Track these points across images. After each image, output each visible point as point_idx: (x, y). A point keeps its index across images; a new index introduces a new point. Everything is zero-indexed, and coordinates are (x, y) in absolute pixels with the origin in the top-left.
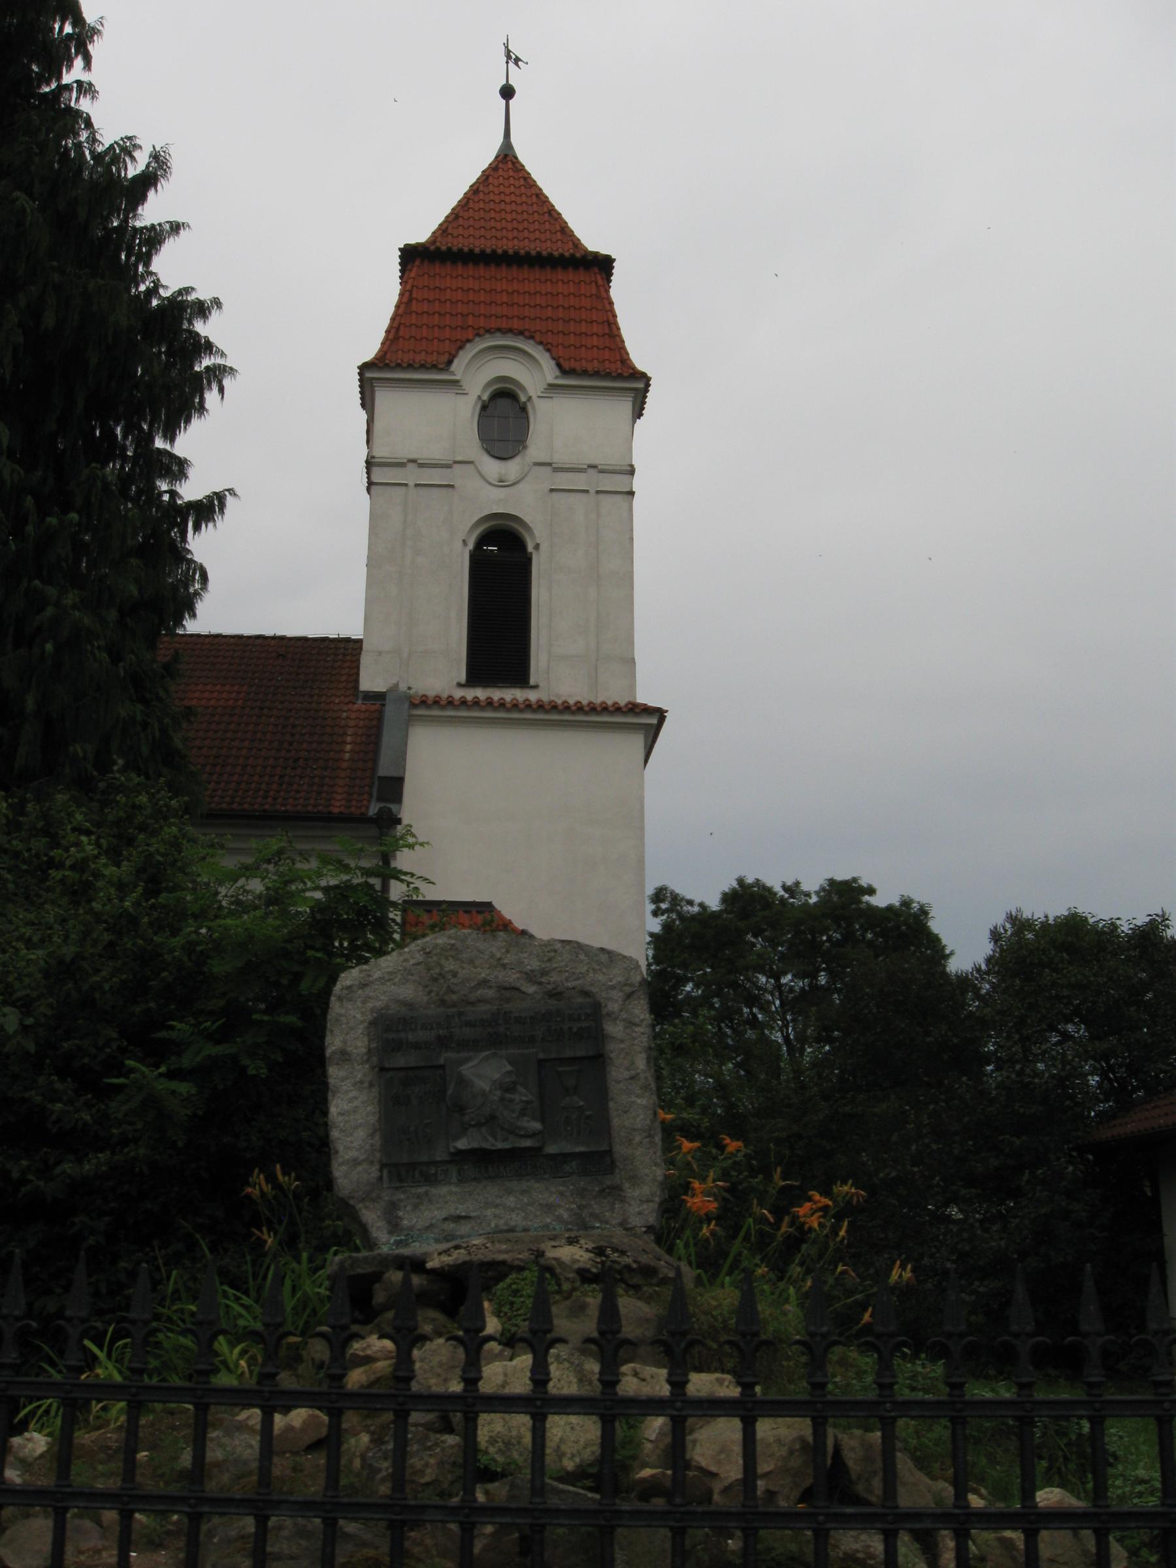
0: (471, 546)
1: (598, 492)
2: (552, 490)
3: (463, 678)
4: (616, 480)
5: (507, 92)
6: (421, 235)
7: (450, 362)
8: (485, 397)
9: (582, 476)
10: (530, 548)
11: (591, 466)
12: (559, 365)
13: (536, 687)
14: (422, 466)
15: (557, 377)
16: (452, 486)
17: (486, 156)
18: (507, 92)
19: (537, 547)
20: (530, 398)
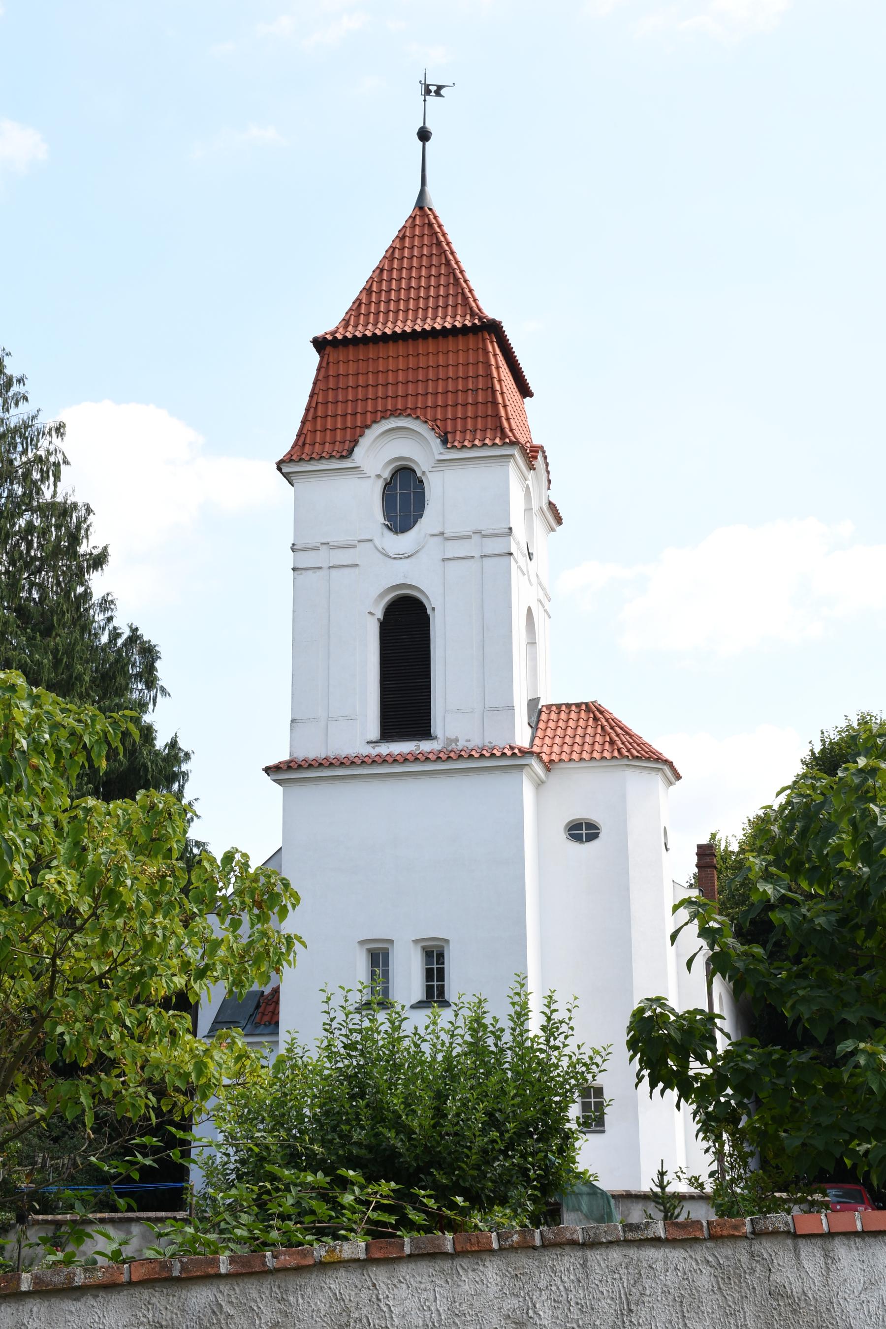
0: (379, 614)
1: (482, 557)
2: (443, 560)
3: (374, 731)
4: (493, 544)
5: (424, 135)
6: (329, 322)
7: (351, 452)
8: (387, 474)
9: (466, 543)
10: (429, 612)
11: (475, 532)
12: (445, 442)
13: (436, 738)
14: (333, 548)
15: (441, 453)
16: (357, 565)
17: (408, 208)
18: (424, 135)
19: (433, 609)
20: (424, 473)
